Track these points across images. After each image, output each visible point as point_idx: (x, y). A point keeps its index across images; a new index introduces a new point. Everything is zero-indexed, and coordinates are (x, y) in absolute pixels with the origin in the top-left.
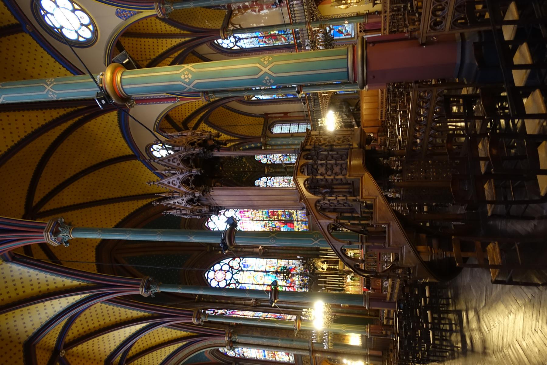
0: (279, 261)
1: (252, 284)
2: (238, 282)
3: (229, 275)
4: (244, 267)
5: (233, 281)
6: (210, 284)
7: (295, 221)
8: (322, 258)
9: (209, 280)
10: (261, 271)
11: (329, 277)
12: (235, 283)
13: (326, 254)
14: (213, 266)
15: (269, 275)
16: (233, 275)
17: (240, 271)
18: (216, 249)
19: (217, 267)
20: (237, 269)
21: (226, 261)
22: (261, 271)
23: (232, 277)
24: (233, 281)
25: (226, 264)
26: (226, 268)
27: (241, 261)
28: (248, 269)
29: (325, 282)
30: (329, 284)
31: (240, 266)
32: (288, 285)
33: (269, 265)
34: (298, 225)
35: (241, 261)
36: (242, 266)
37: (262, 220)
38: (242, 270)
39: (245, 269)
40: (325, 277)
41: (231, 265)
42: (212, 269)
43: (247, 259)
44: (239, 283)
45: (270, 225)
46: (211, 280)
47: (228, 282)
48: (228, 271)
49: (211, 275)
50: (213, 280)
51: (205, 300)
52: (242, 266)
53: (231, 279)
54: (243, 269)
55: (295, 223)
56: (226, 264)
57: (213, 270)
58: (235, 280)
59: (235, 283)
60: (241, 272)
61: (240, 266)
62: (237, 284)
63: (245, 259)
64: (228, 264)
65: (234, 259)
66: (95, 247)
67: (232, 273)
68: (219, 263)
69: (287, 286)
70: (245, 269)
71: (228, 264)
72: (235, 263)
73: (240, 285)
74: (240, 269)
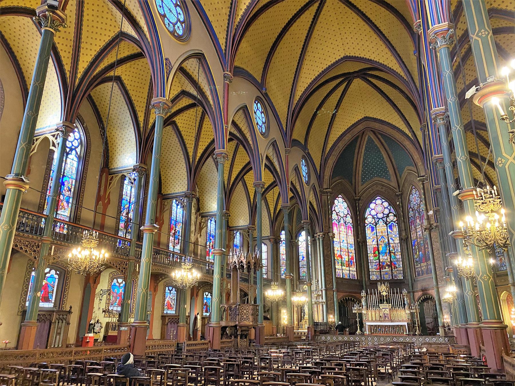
0: (400, 253)
1: (377, 236)
2: (376, 224)
3: (380, 216)
4: (389, 226)
5: (377, 220)
6: (371, 203)
7: (427, 264)
8: (390, 290)
9: (374, 202)
10: (389, 241)
11: (376, 296)
12: (375, 222)
13: (394, 293)
14: (386, 201)
15: (386, 247)
16: (382, 219)
17: (386, 223)
18: (400, 199)
19: (386, 204)
20: (387, 221)
21: (392, 210)
22: (389, 241)
23: (379, 219)
24: (377, 220)
25: (390, 210)
26: (386, 211)
27: (394, 222)
28: (389, 230)
29: (371, 294)
30: (370, 297)
31: (390, 222)
32: (381, 263)
33: (394, 246)
34: (425, 266)
35: (394, 222)
36: (390, 224)
37: (423, 234)
38: (387, 225)
39: (388, 227)
40: (375, 294)
41: (390, 215)
42: (383, 201)
43: (397, 227)
44: (376, 226)
45: (421, 242)
46: (375, 203)
47: (376, 217)
48: (384, 214)
49: (379, 202)
50: (375, 205)
51: (357, 204)
52: (390, 224)
53: (378, 218)
54: (388, 225)
55: (425, 264)
56: (390, 210)
57: (382, 203)
58: (378, 221)
59: (375, 222)
60: (385, 225)
61: (390, 222)
62: (375, 224)
63: (397, 225)
64: (390, 213)
65: (395, 216)
66: (365, 116)
67: (383, 218)
68: (389, 205)
69: (380, 263)
70: (388, 227)
71: (390, 213)
72: (391, 217)
73: (374, 226)
74: (387, 223)
